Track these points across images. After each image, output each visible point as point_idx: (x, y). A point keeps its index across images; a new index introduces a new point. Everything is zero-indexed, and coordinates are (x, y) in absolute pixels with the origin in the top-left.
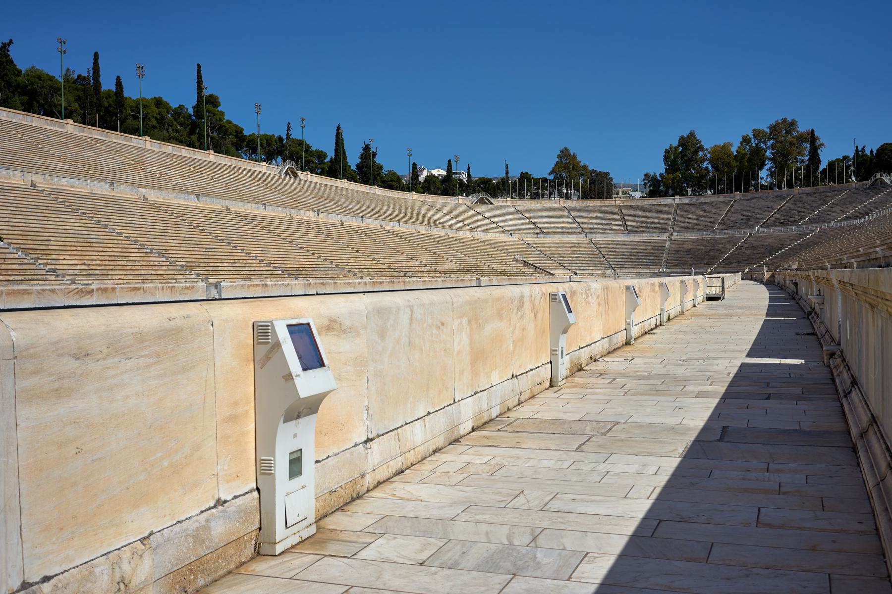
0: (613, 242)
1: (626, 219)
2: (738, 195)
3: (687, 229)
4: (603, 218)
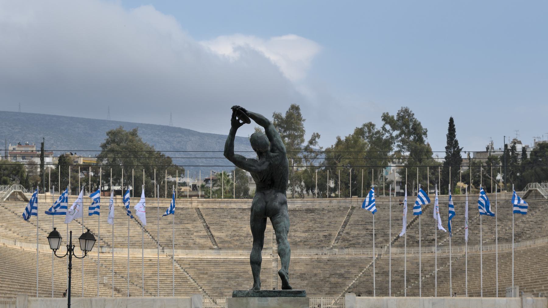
0: (201, 260)
1: (211, 227)
2: (355, 201)
4: (181, 226)
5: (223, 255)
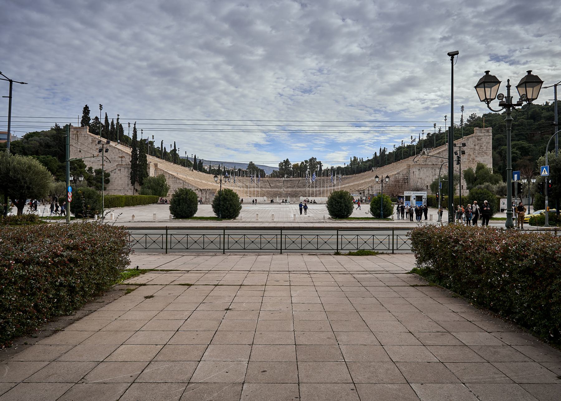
2: (300, 178)
3: (288, 187)
5: (273, 190)
